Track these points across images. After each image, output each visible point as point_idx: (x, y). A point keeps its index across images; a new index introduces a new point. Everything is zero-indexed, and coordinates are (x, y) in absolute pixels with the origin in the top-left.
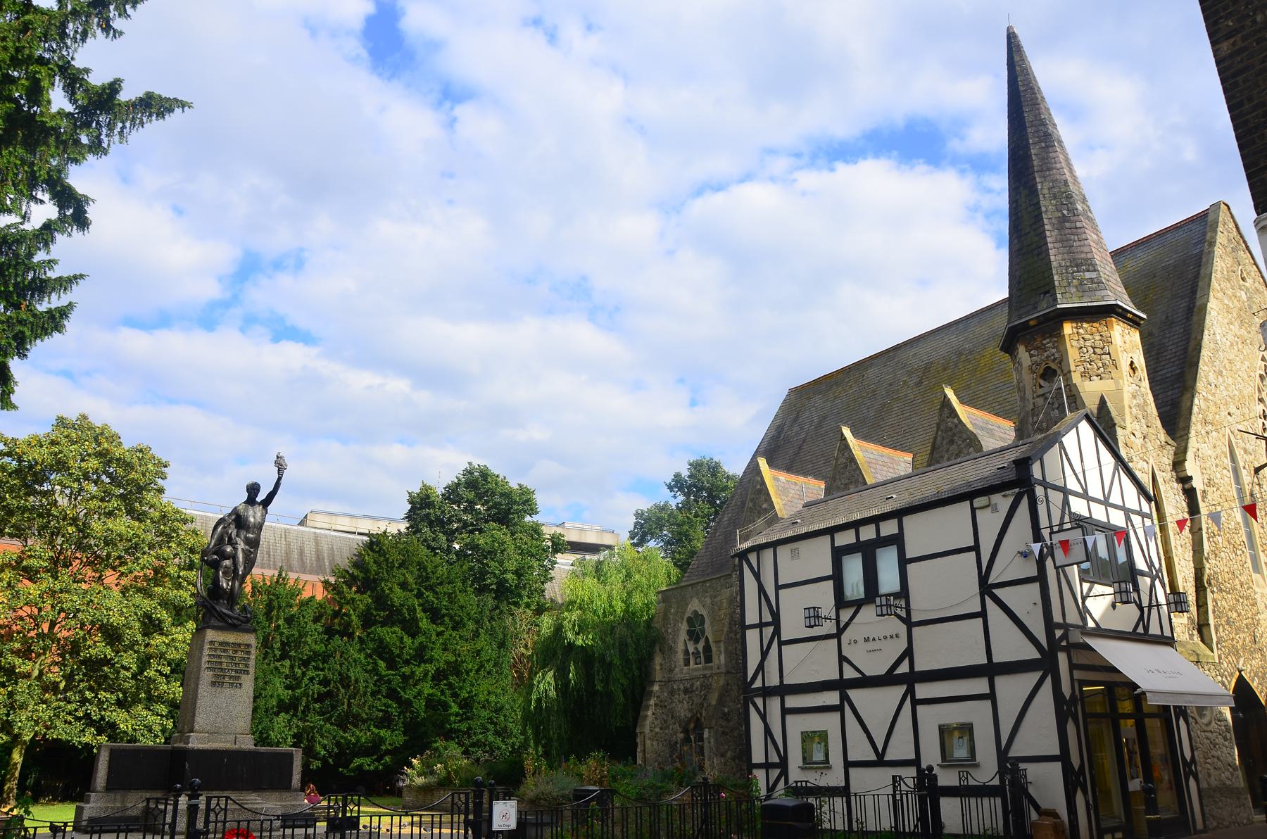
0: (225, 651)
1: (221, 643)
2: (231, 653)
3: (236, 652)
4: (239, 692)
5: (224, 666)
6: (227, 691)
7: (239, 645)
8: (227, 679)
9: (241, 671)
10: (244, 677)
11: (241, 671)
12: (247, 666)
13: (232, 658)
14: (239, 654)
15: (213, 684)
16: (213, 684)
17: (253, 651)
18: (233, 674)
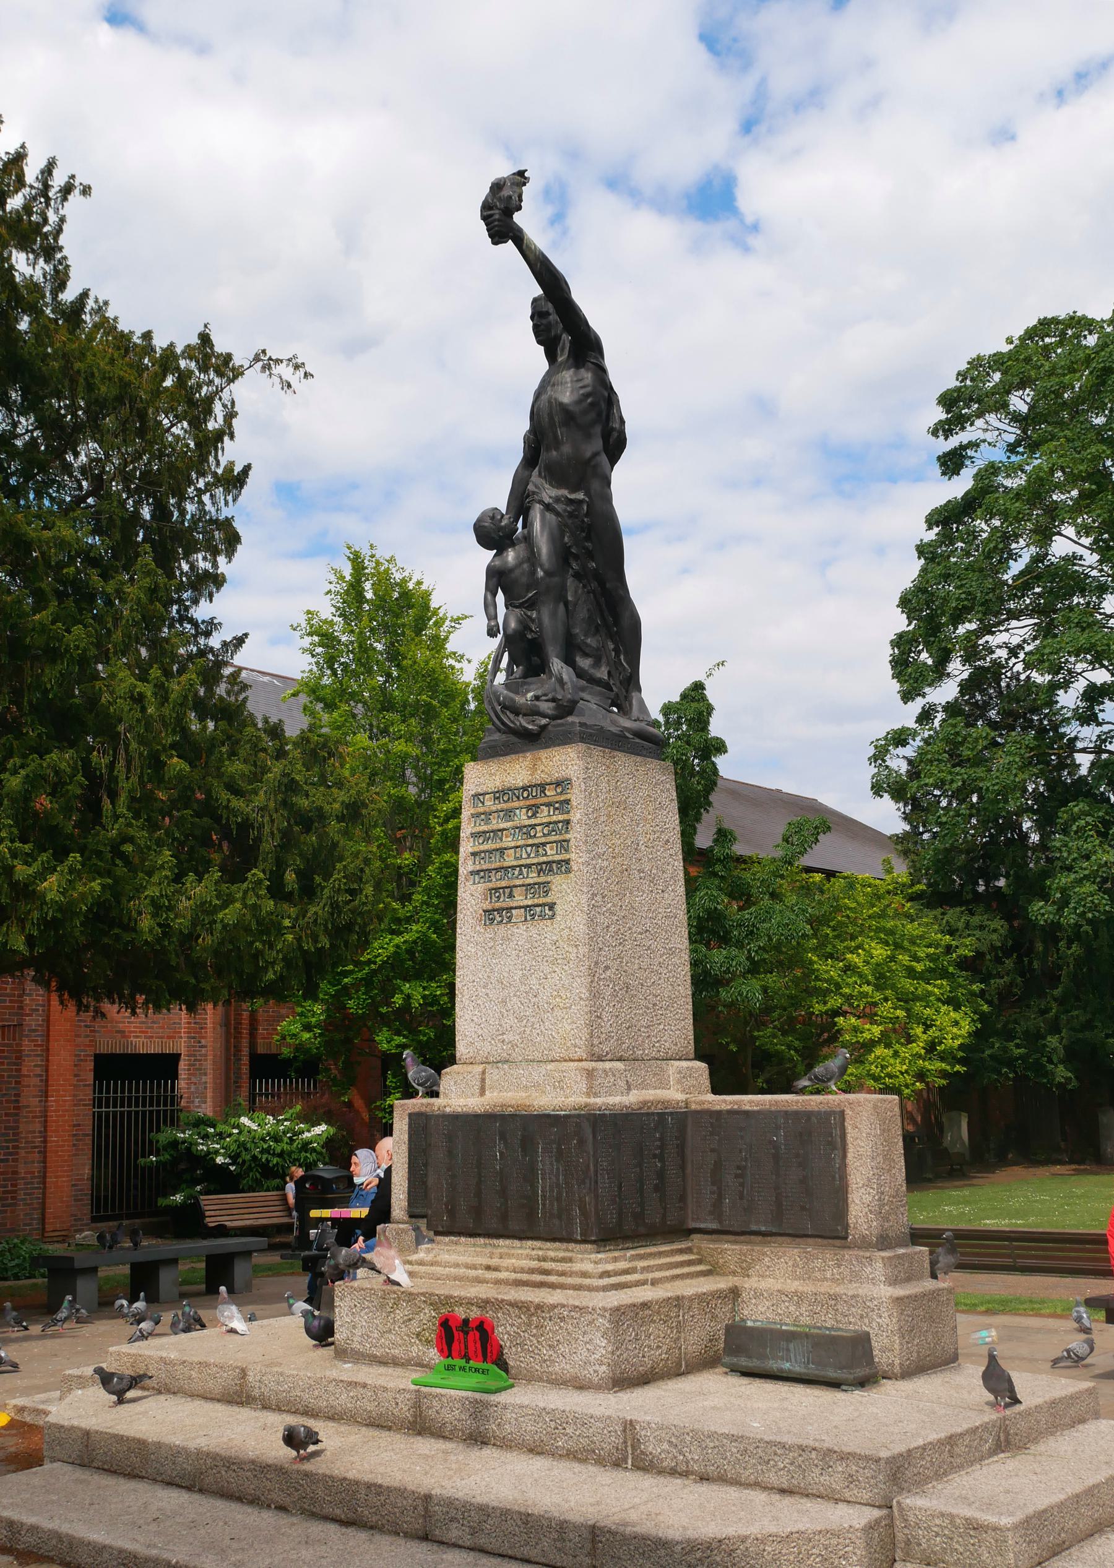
0: (509, 814)
1: (499, 794)
2: (522, 817)
3: (534, 809)
4: (546, 932)
5: (510, 861)
6: (521, 932)
7: (542, 787)
8: (520, 899)
9: (546, 868)
10: (558, 882)
11: (546, 868)
12: (564, 845)
13: (527, 830)
14: (544, 815)
15: (491, 916)
16: (491, 916)
17: (576, 796)
18: (533, 877)
